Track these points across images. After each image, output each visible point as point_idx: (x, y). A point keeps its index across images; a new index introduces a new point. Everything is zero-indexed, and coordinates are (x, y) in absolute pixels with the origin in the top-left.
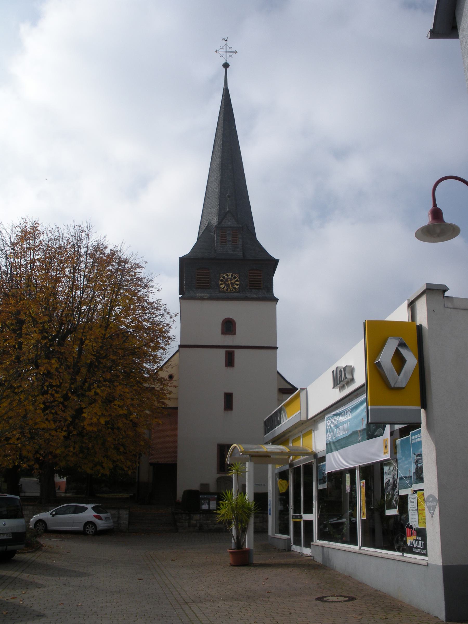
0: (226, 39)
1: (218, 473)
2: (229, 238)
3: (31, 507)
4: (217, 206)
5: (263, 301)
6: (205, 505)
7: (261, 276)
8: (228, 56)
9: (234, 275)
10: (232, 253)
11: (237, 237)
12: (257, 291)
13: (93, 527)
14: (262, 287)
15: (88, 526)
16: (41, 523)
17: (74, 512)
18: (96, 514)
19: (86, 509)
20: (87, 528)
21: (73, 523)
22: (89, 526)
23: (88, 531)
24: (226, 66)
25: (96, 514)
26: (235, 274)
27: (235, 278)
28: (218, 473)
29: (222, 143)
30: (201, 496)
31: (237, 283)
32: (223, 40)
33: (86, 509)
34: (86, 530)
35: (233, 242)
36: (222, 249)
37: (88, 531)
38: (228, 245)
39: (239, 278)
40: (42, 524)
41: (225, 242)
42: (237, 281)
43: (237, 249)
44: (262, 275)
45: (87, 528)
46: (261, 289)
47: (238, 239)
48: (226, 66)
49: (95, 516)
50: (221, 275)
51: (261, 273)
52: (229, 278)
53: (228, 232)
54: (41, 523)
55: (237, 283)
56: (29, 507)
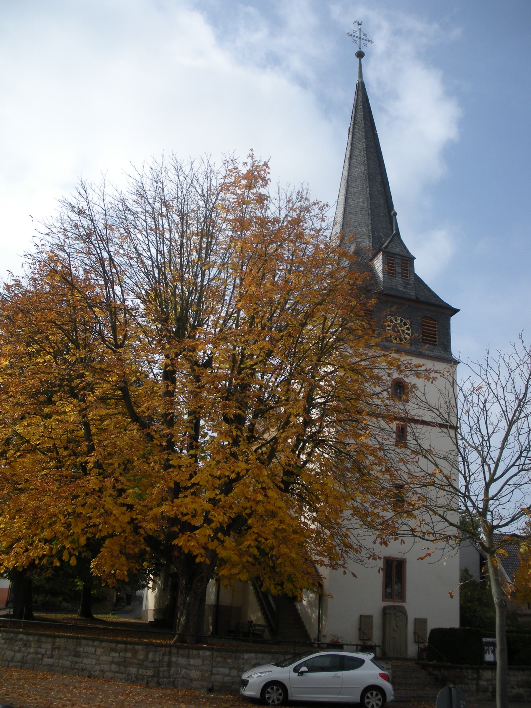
0: (360, 23)
1: (383, 600)
2: (399, 269)
3: (208, 653)
4: (368, 225)
5: (440, 362)
6: (489, 653)
7: (435, 328)
8: (362, 45)
9: (404, 320)
10: (403, 290)
11: (407, 270)
12: (432, 347)
13: (380, 696)
14: (437, 343)
15: (369, 695)
16: (275, 688)
17: (342, 668)
18: (381, 672)
19: (361, 662)
20: (368, 698)
21: (341, 688)
22: (372, 694)
23: (368, 703)
24: (360, 55)
25: (381, 672)
26: (405, 318)
27: (405, 324)
28: (383, 600)
29: (366, 147)
30: (484, 640)
31: (407, 331)
32: (355, 22)
33: (361, 662)
34: (269, 690)
35: (403, 276)
36: (389, 281)
37: (368, 703)
38: (397, 278)
39: (410, 325)
40: (278, 690)
41: (393, 274)
42: (408, 329)
43: (409, 286)
44: (436, 326)
45: (368, 698)
46: (436, 345)
47: (408, 272)
48: (360, 55)
49: (382, 675)
50: (388, 317)
51: (435, 324)
52: (398, 324)
53: (397, 261)
54: (275, 688)
55: (407, 331)
56: (201, 652)
